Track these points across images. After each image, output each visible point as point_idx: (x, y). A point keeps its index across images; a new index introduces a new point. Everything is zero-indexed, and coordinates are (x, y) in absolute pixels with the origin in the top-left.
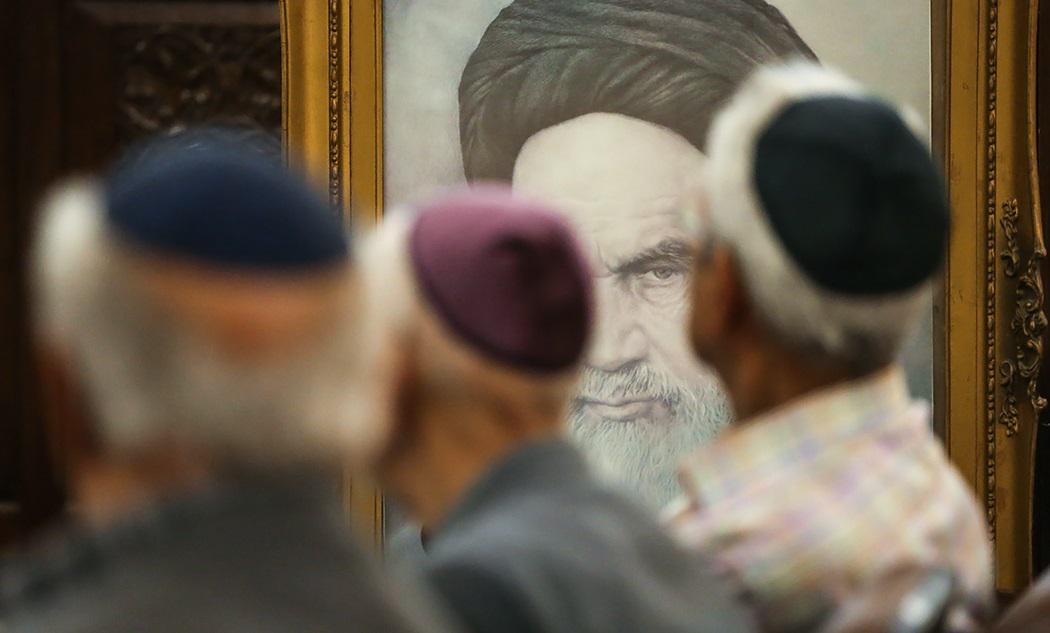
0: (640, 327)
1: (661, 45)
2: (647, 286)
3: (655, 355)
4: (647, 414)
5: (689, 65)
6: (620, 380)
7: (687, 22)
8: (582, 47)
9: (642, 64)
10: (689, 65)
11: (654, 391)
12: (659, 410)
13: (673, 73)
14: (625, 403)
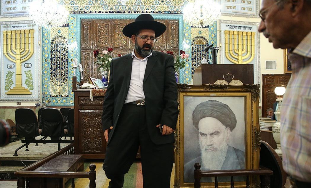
0: (213, 141)
1: (215, 109)
2: (213, 136)
3: (214, 144)
4: (214, 150)
5: (218, 111)
6: (210, 147)
7: (218, 107)
8: (206, 109)
9: (213, 111)
10: (218, 111)
11: (214, 148)
12: (215, 150)
13: (216, 112)
14: (211, 149)
